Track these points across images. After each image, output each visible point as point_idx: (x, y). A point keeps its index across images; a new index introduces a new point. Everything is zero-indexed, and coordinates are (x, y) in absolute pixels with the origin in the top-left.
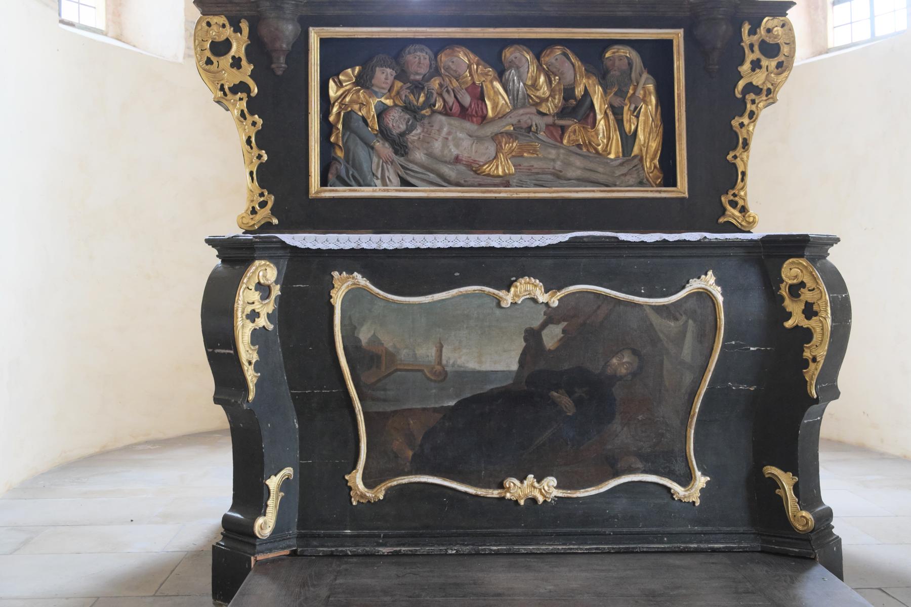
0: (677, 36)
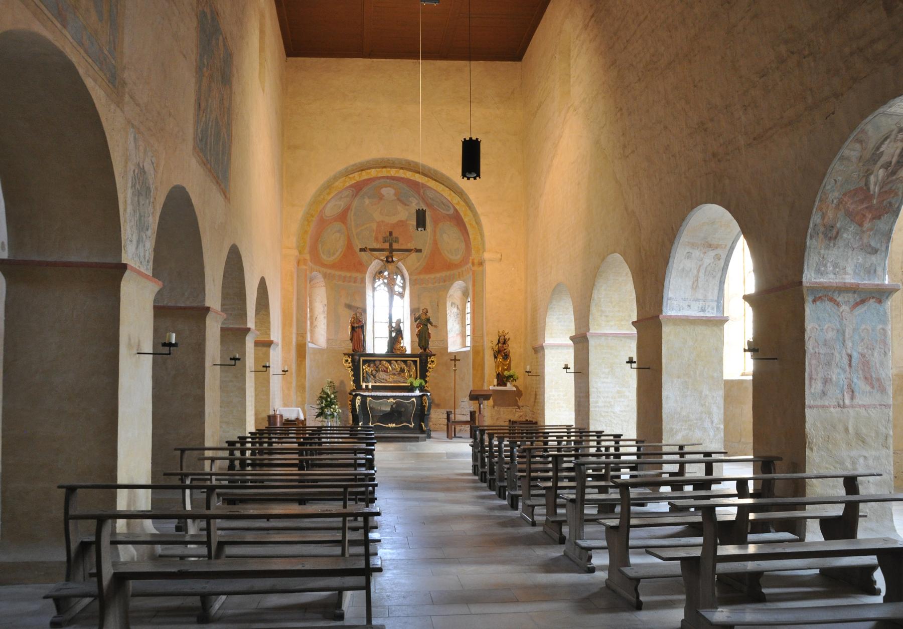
0: (418, 359)
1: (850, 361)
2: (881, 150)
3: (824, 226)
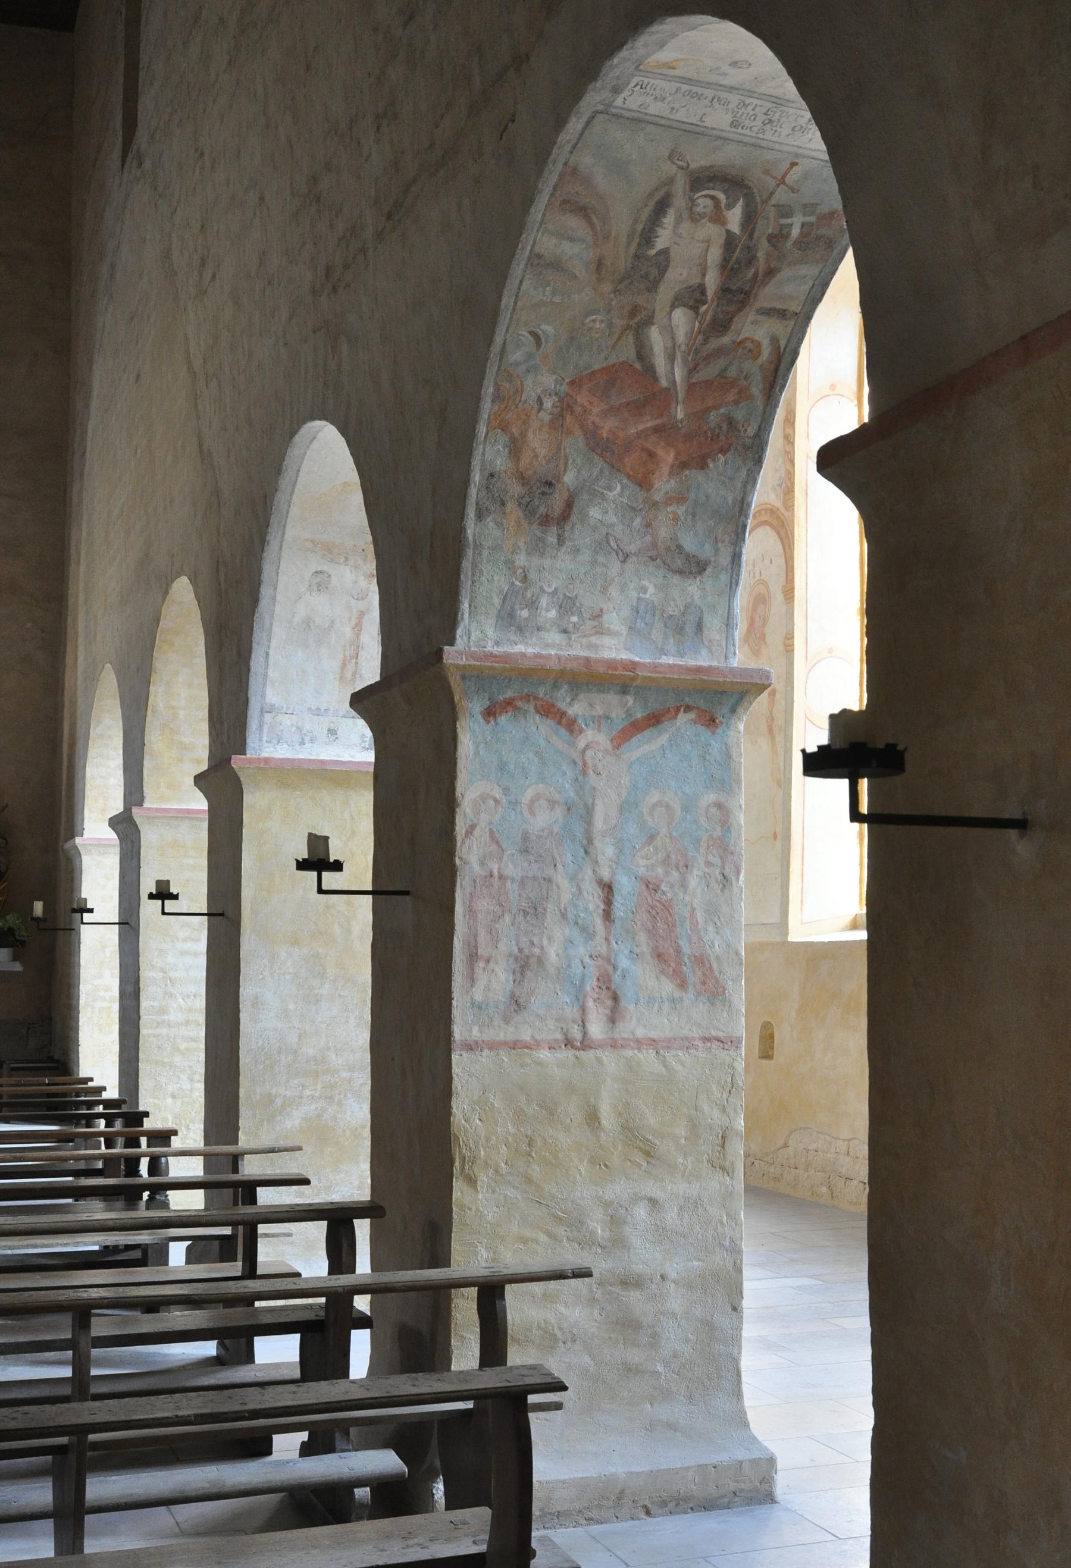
1: (608, 902)
2: (660, 244)
3: (523, 479)
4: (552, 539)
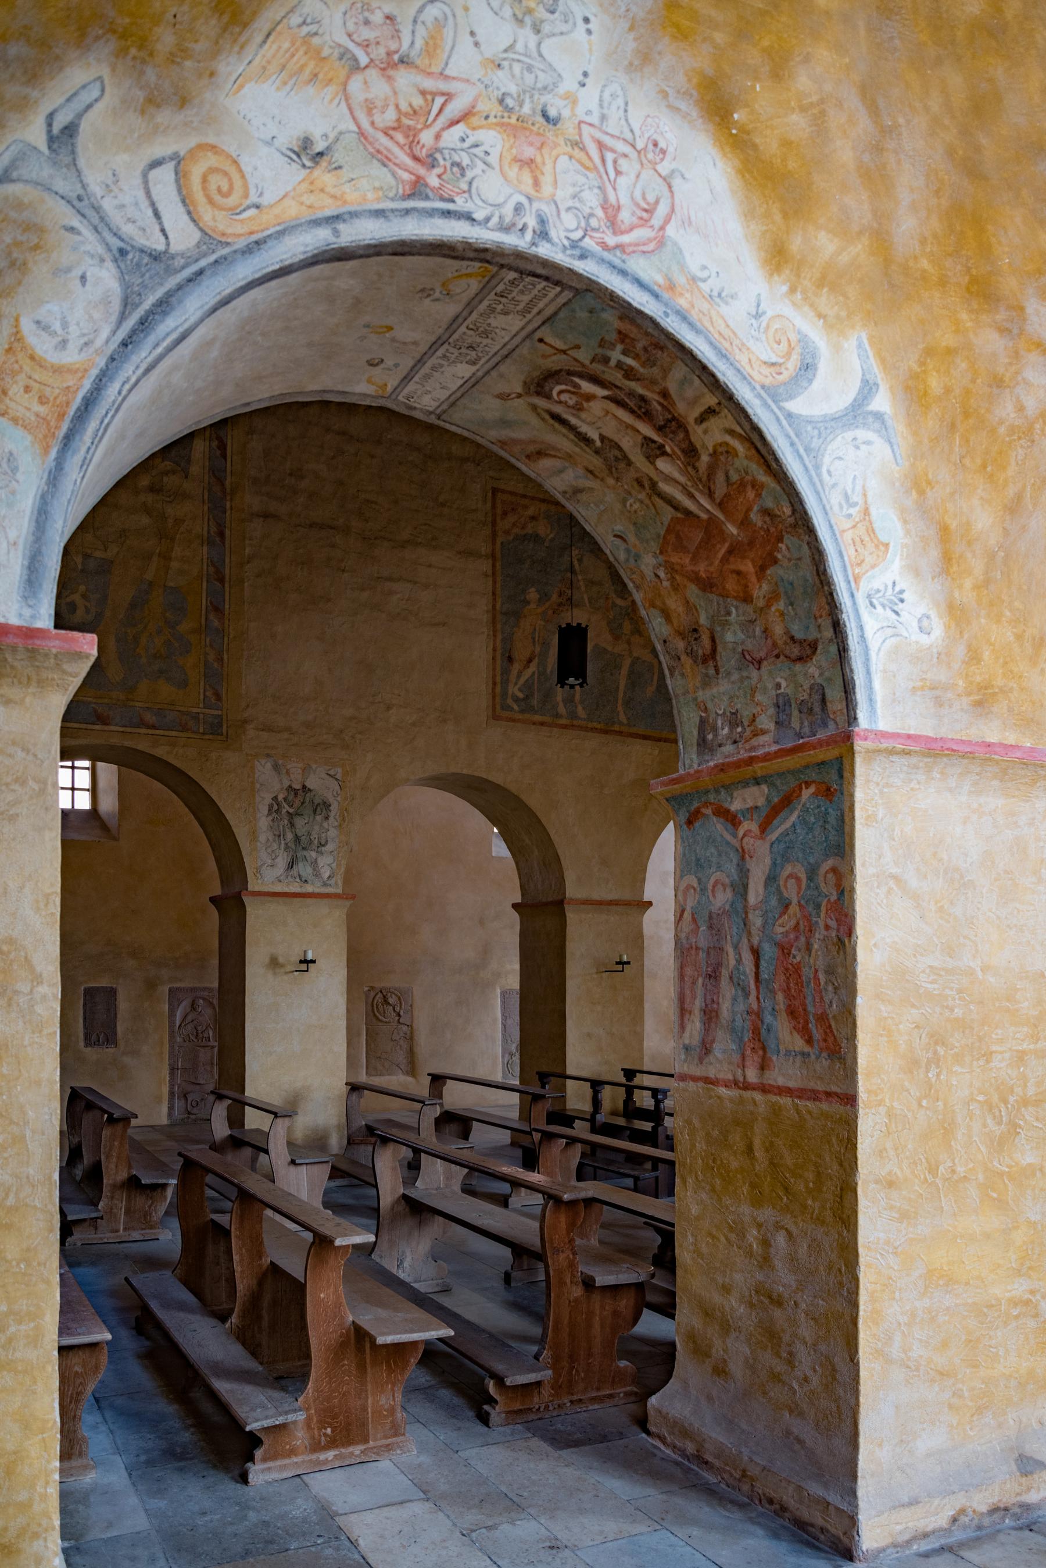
2: (594, 435)
3: (681, 634)
4: (712, 672)
